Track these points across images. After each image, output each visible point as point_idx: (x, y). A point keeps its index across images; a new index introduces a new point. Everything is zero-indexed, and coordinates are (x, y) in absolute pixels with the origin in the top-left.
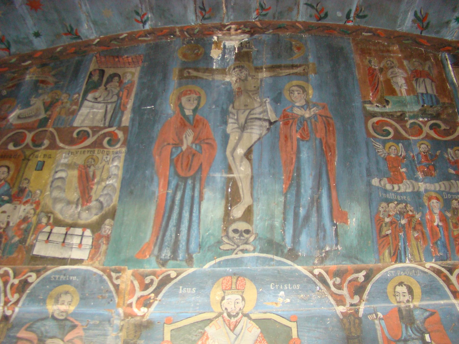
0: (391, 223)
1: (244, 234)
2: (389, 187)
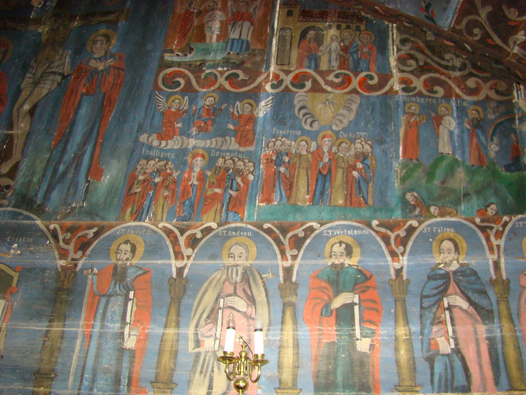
0: (144, 181)
1: (4, 189)
2: (156, 143)
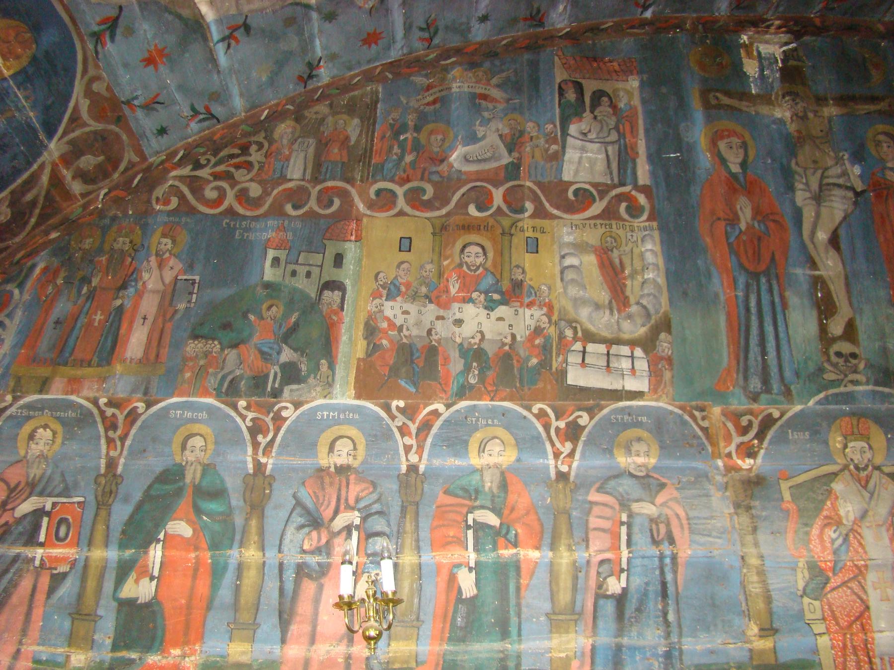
1: (851, 359)
